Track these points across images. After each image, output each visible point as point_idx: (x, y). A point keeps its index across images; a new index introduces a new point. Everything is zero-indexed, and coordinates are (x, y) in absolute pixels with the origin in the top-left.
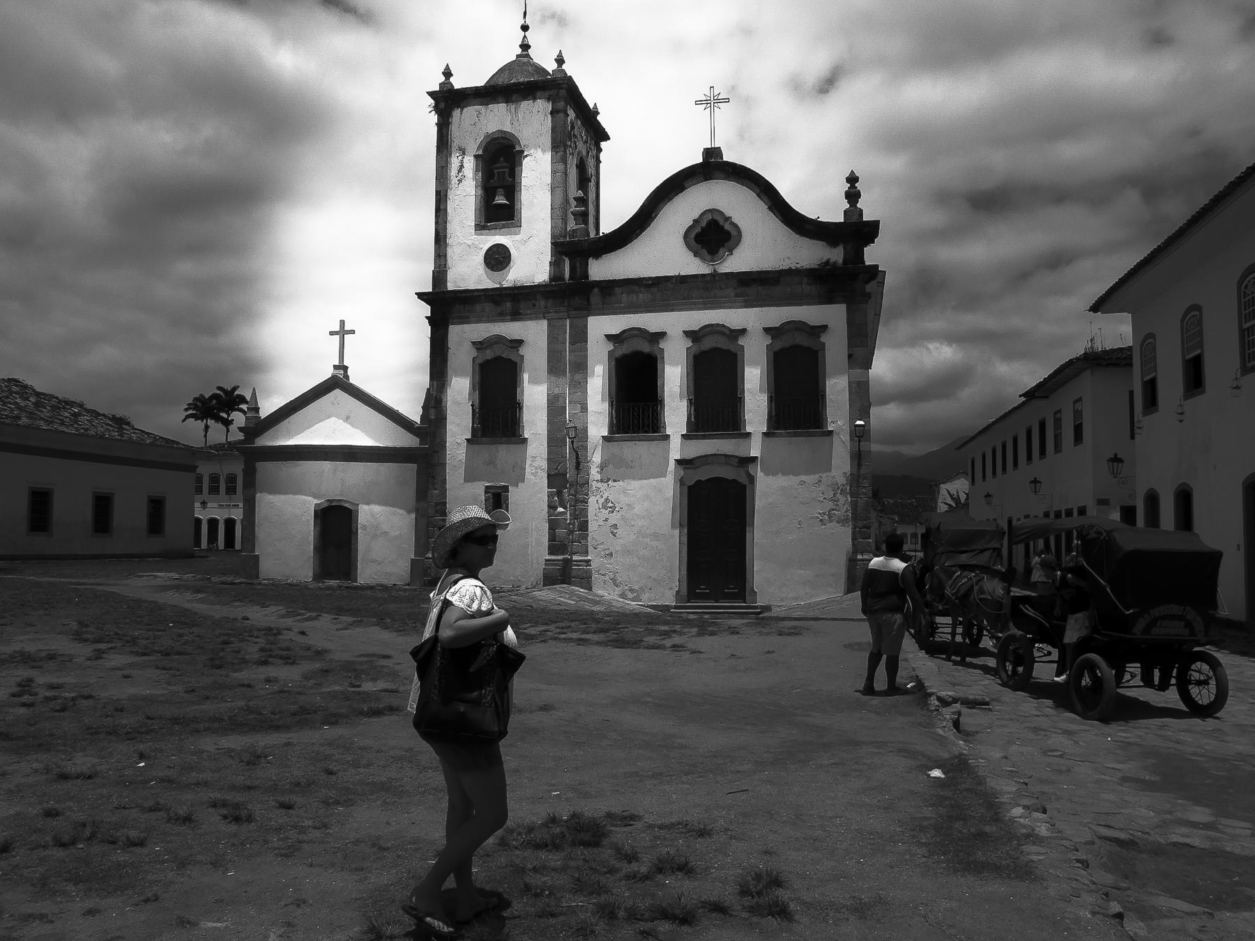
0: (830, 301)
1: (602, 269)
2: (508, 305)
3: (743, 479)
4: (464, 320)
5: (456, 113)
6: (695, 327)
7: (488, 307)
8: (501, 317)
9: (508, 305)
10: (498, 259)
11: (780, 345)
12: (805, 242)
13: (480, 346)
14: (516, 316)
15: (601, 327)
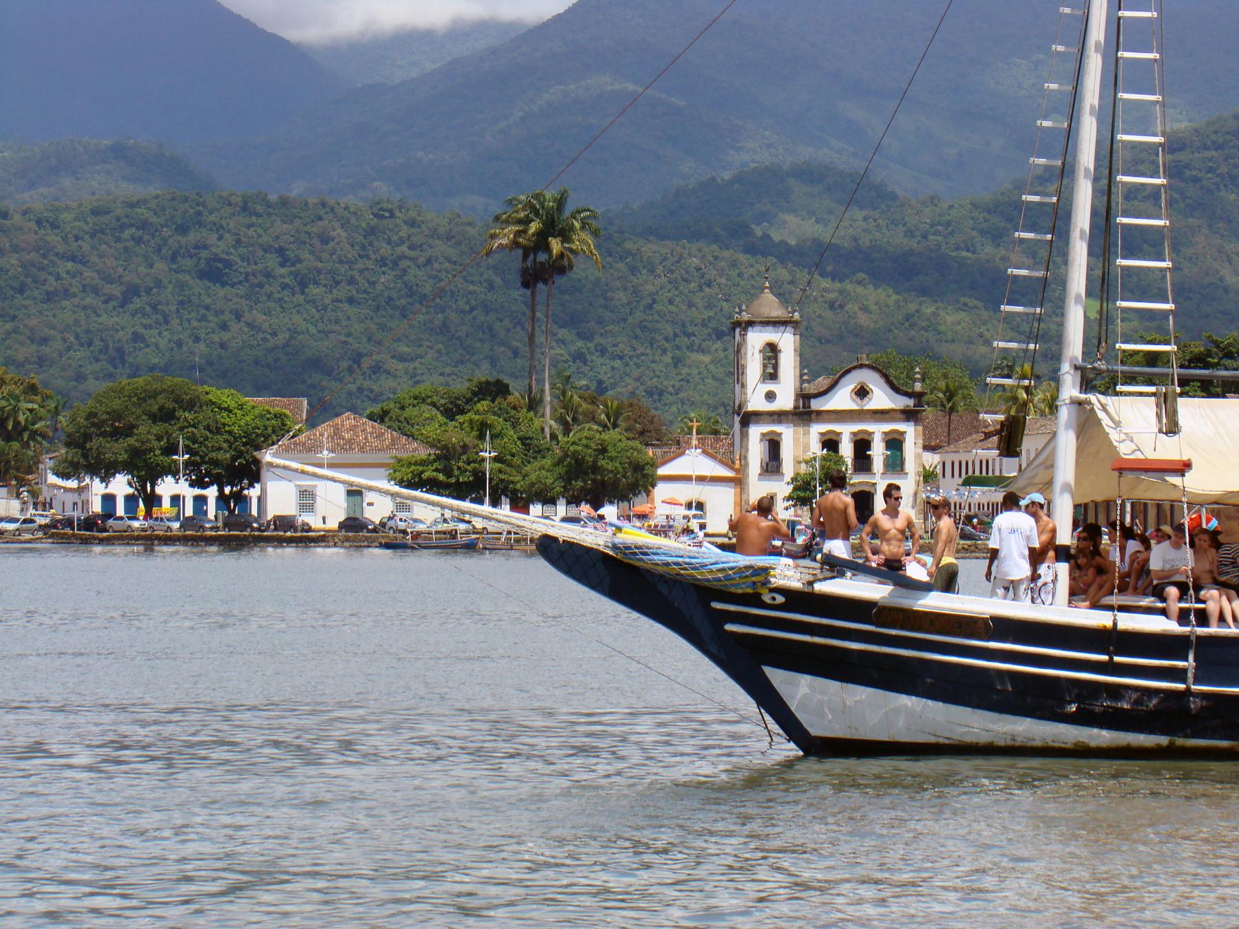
0: (908, 421)
1: (816, 405)
2: (776, 417)
3: (872, 491)
4: (757, 422)
5: (750, 329)
6: (856, 430)
7: (768, 417)
8: (773, 422)
9: (776, 417)
10: (770, 396)
11: (888, 438)
12: (899, 397)
13: (763, 435)
14: (780, 422)
15: (817, 430)
